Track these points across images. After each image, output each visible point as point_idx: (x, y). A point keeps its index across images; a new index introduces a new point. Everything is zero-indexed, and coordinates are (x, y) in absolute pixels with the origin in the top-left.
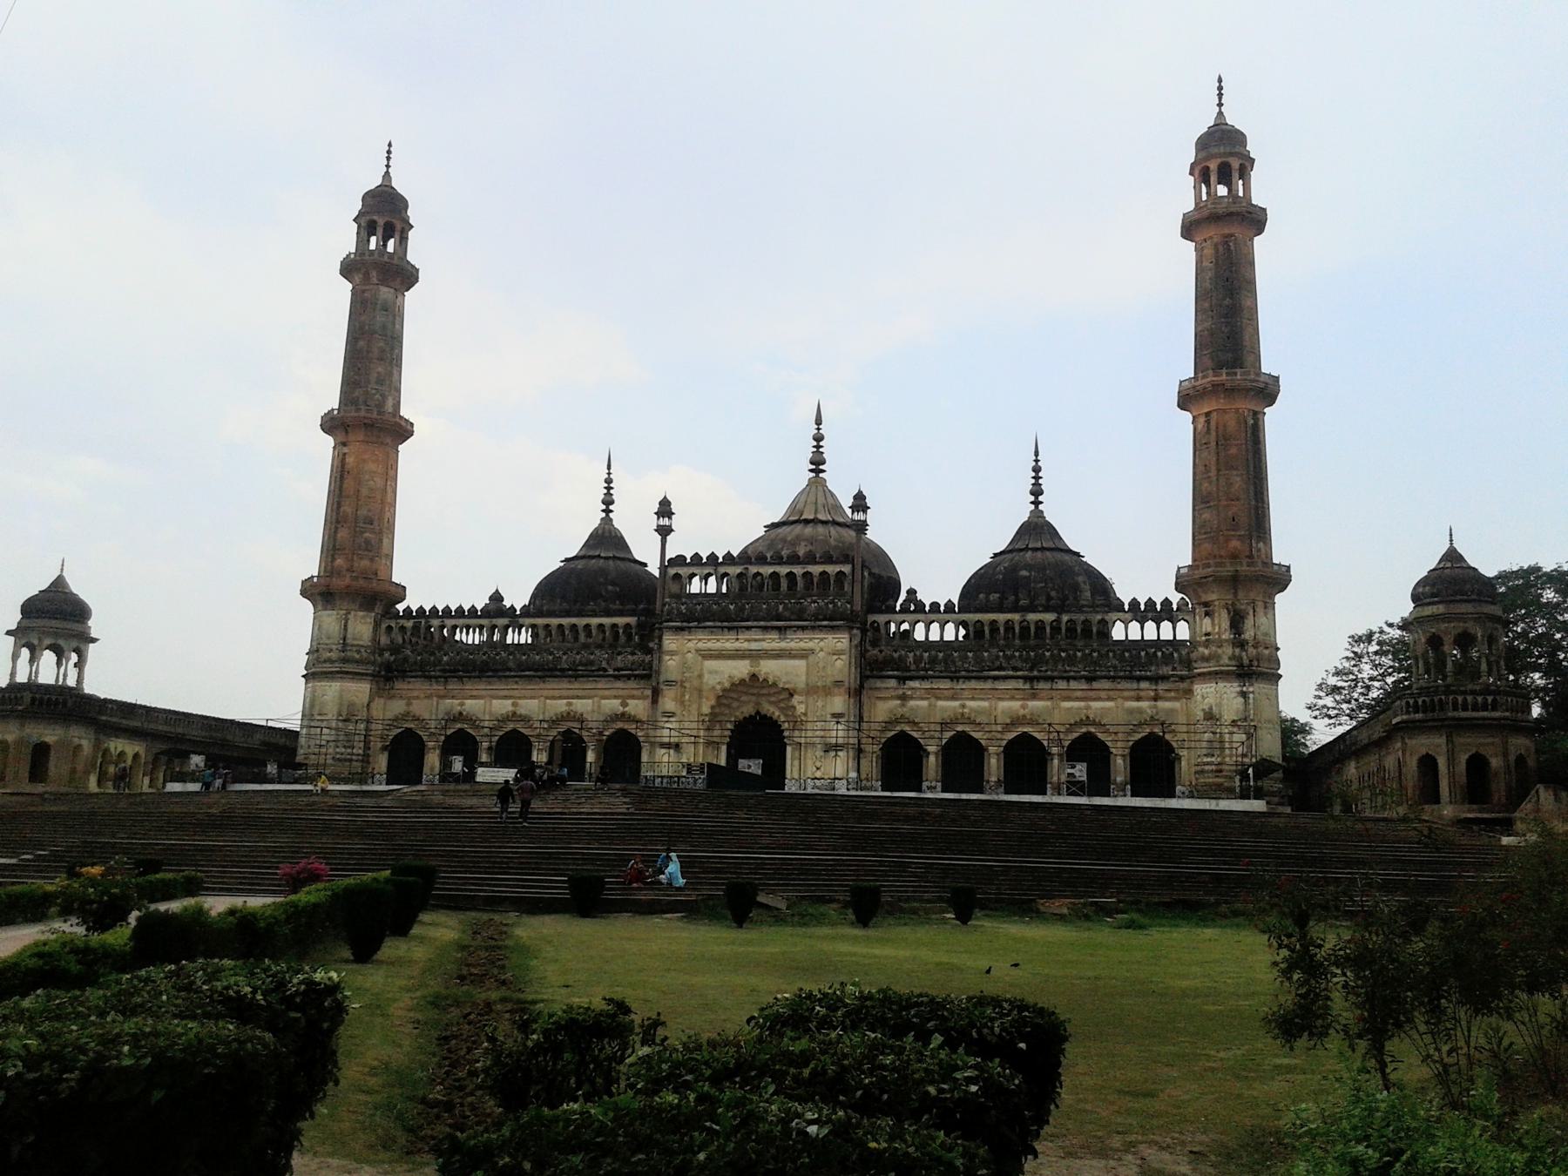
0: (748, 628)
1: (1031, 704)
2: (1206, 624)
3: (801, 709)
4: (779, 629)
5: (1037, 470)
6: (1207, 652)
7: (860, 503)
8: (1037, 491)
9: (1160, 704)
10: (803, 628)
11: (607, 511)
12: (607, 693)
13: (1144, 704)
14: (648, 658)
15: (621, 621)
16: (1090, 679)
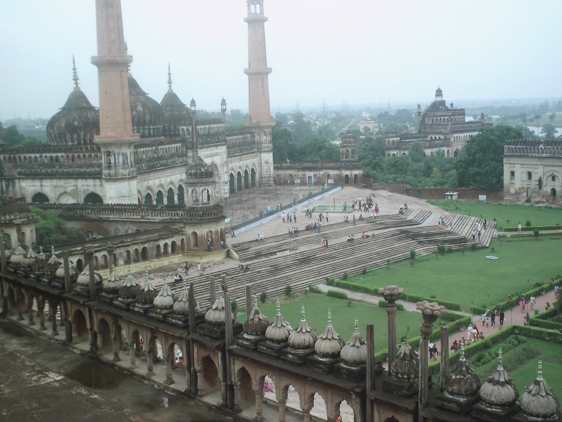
0: (212, 146)
1: (241, 162)
2: (265, 137)
3: (220, 172)
4: (216, 146)
5: (169, 74)
6: (265, 145)
7: (223, 102)
8: (170, 82)
9: (255, 159)
10: (220, 145)
11: (77, 84)
12: (177, 172)
13: (252, 160)
14: (184, 158)
15: (179, 145)
16: (247, 154)
